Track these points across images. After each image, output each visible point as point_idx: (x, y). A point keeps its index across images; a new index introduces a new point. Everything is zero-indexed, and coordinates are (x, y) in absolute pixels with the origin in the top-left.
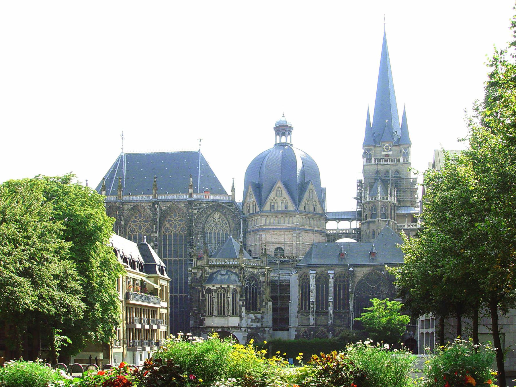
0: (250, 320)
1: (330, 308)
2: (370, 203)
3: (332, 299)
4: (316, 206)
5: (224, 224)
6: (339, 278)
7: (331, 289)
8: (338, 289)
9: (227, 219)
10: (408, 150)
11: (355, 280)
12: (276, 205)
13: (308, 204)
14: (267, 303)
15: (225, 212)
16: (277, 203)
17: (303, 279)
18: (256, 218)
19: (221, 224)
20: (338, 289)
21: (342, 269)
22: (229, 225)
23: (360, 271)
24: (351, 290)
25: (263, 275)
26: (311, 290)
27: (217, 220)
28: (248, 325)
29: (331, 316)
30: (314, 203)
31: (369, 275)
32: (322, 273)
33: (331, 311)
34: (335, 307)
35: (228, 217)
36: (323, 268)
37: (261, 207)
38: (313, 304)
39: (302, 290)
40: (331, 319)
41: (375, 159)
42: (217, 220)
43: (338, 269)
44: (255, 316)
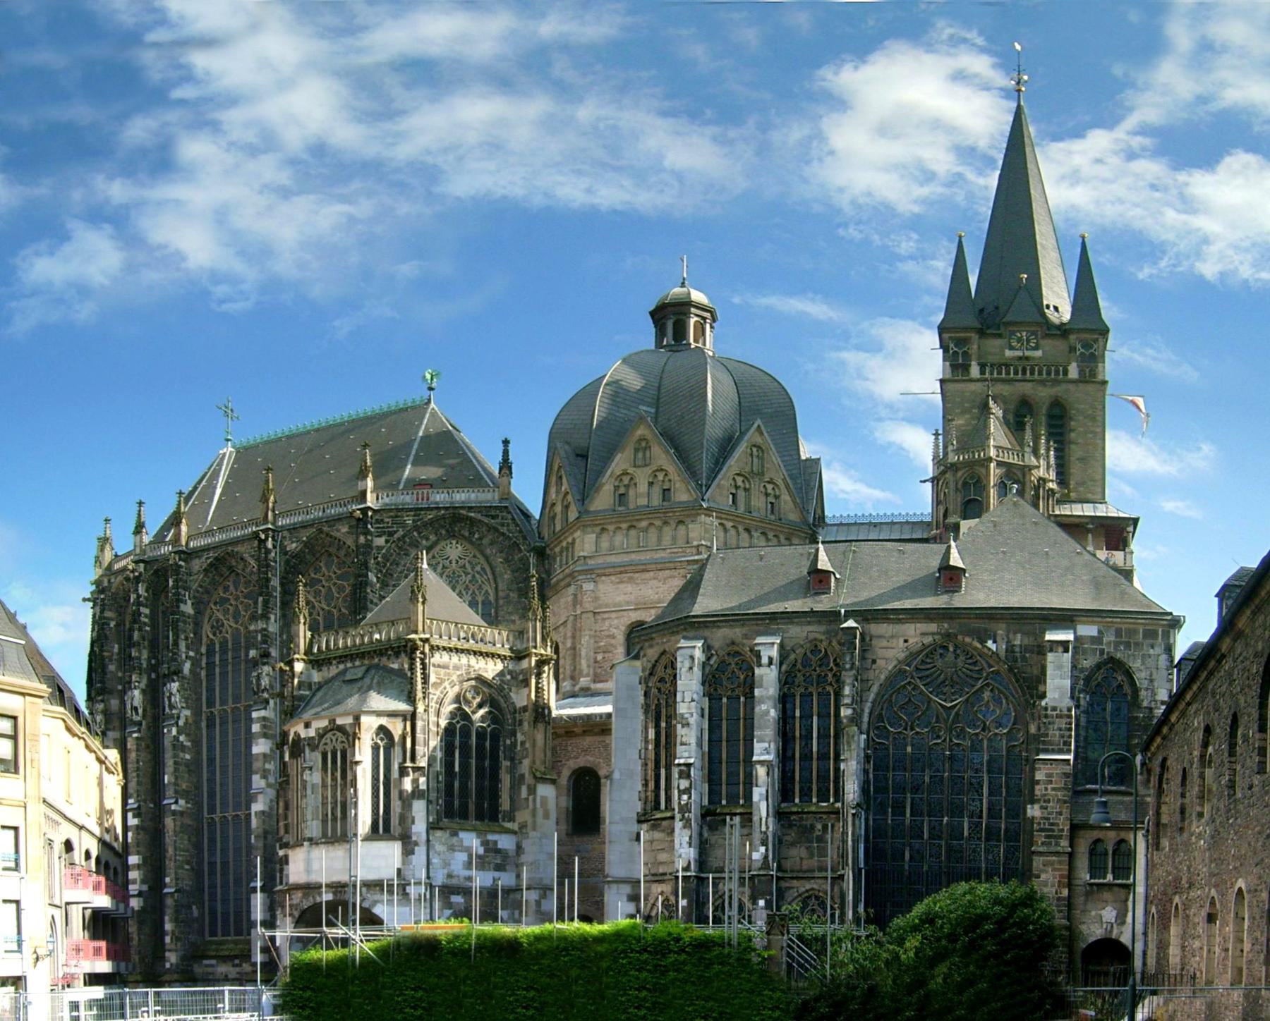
0: (463, 857)
1: (758, 793)
2: (957, 470)
3: (768, 753)
4: (776, 497)
5: (478, 573)
6: (804, 666)
7: (764, 707)
8: (798, 714)
9: (487, 558)
10: (1095, 346)
11: (871, 675)
12: (631, 492)
13: (745, 489)
14: (532, 791)
15: (480, 539)
16: (636, 484)
17: (662, 680)
18: (570, 540)
19: (467, 574)
20: (798, 714)
21: (815, 631)
22: (493, 573)
23: (892, 637)
24: (849, 712)
25: (522, 681)
26: (682, 715)
27: (454, 562)
28: (450, 876)
29: (764, 829)
30: (770, 487)
31: (929, 652)
32: (736, 648)
33: (763, 806)
34: (785, 790)
35: (488, 551)
36: (737, 630)
37: (583, 498)
38: (689, 776)
39: (657, 726)
40: (764, 843)
41: (982, 367)
42: (454, 562)
43: (798, 633)
44: (485, 843)
